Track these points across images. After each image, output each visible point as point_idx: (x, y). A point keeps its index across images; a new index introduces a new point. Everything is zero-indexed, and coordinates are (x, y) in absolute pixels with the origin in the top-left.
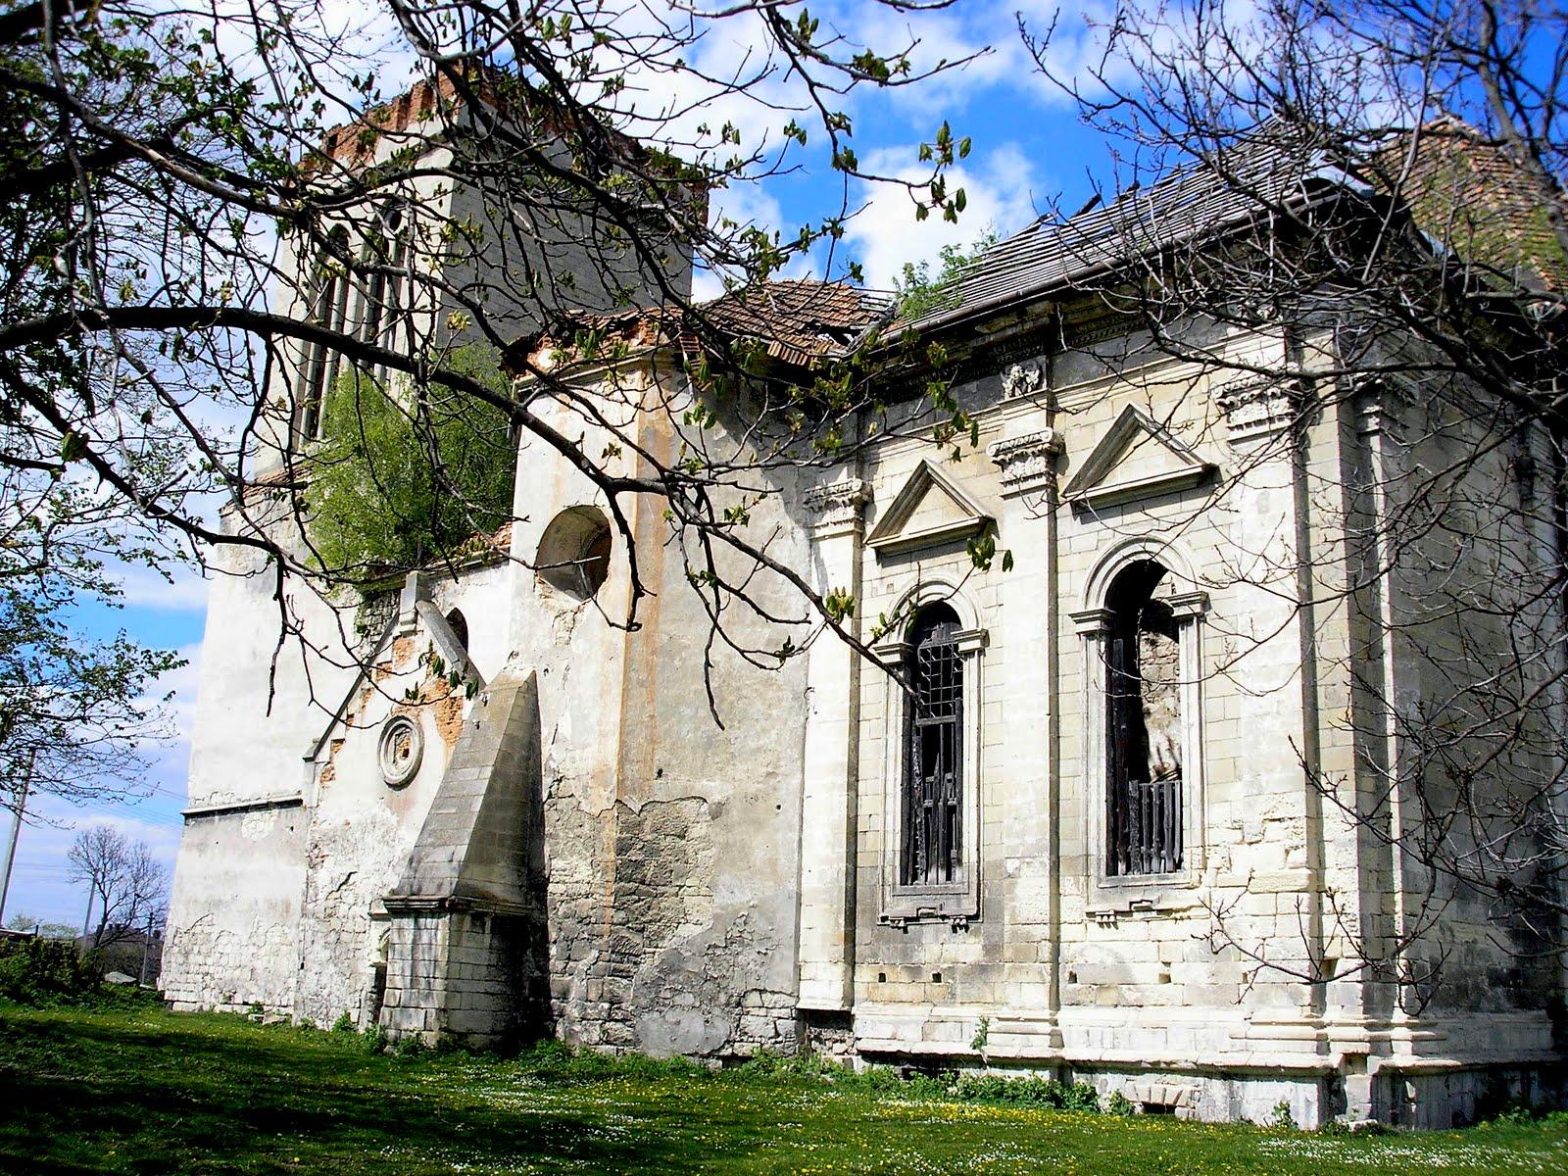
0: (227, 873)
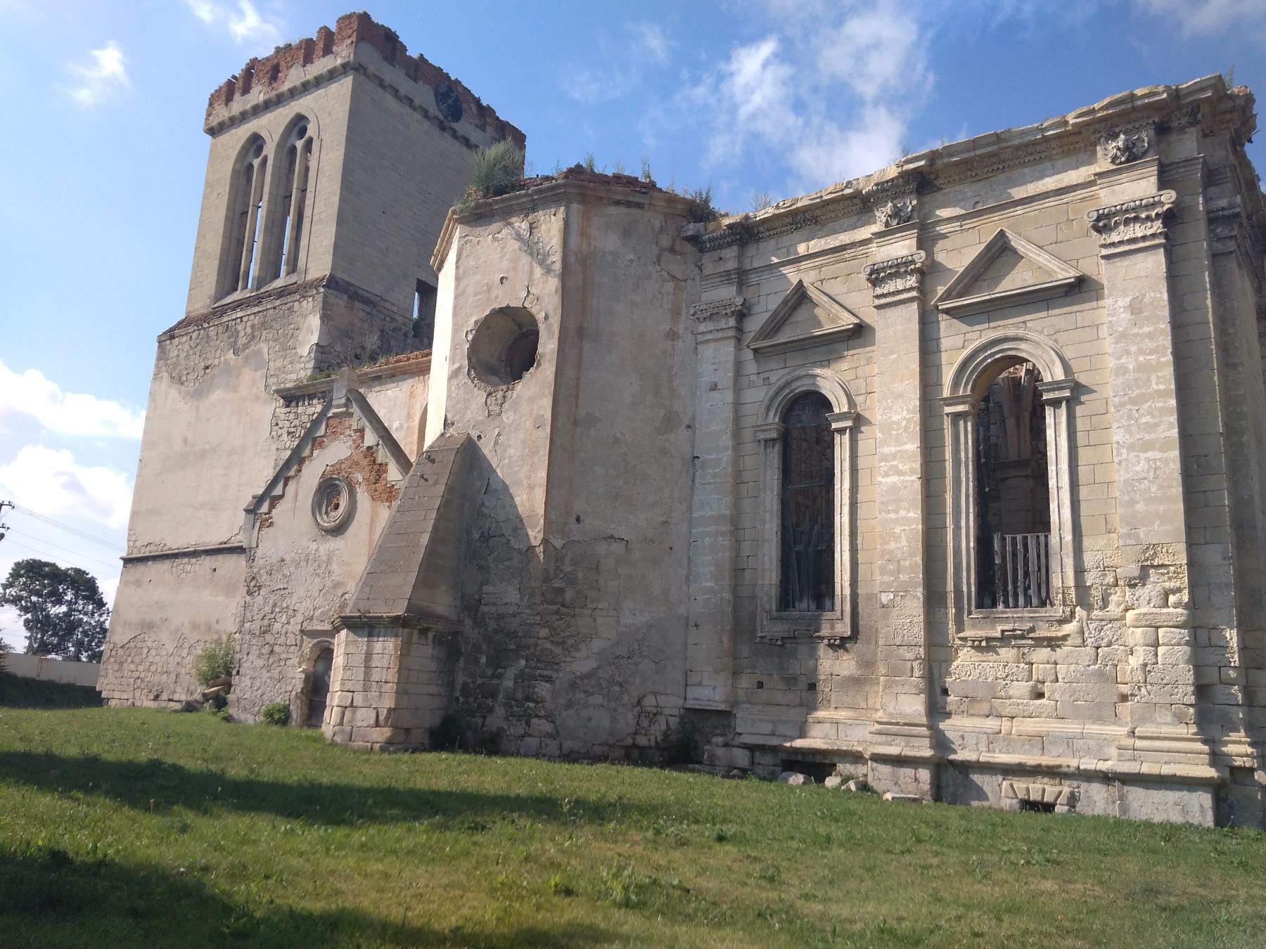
0: (157, 603)
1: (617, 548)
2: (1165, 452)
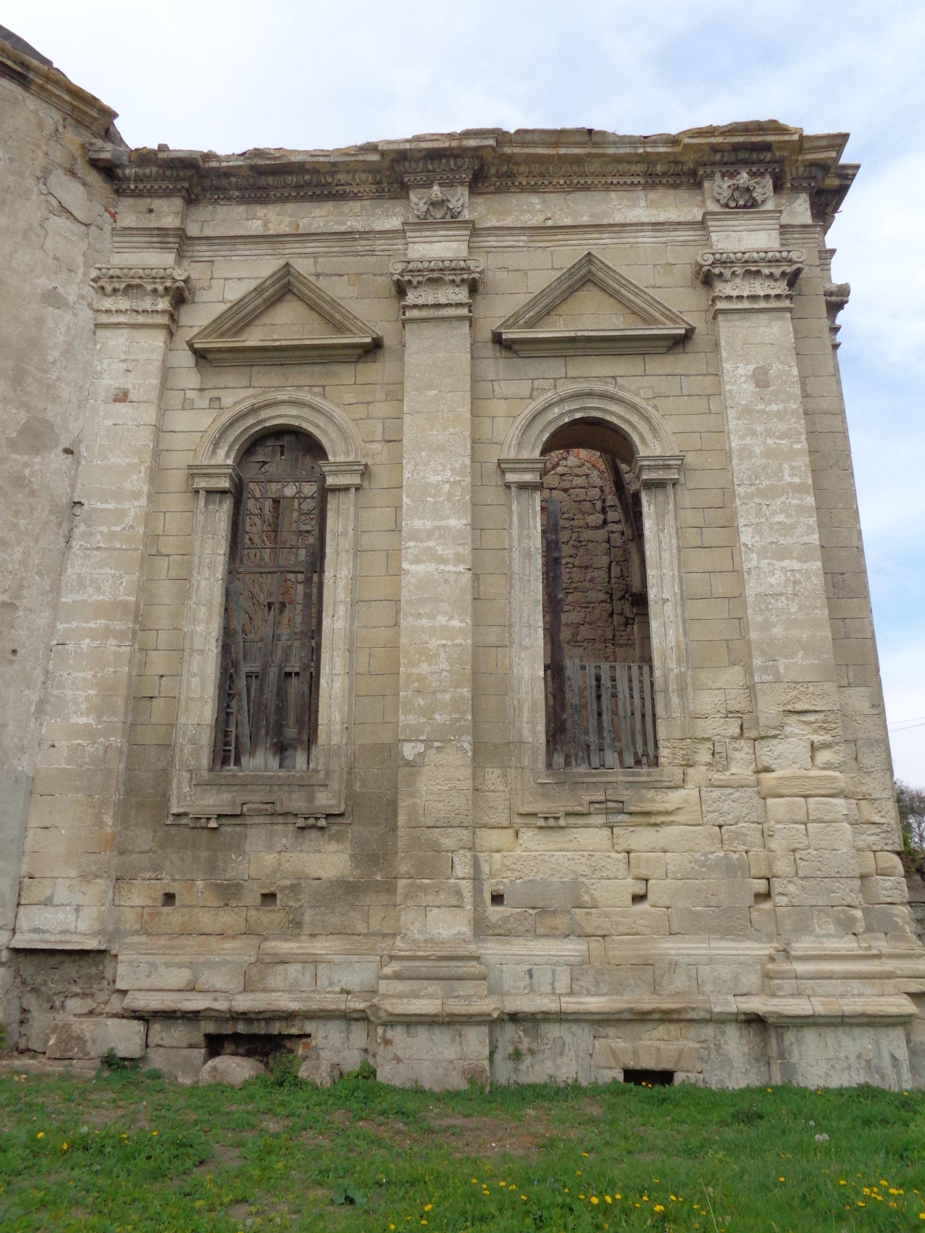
2: (805, 562)
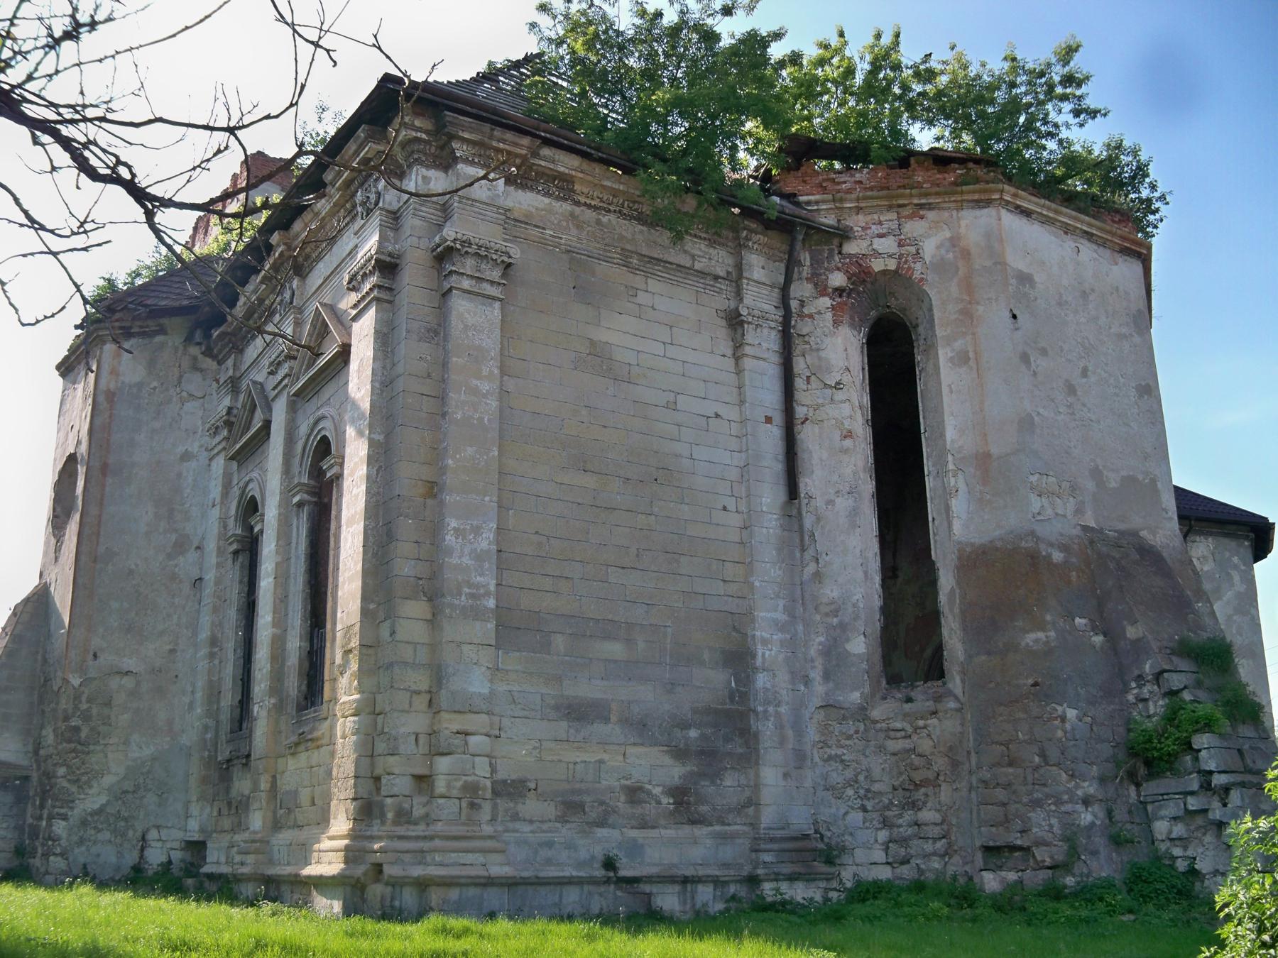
1: (128, 682)
